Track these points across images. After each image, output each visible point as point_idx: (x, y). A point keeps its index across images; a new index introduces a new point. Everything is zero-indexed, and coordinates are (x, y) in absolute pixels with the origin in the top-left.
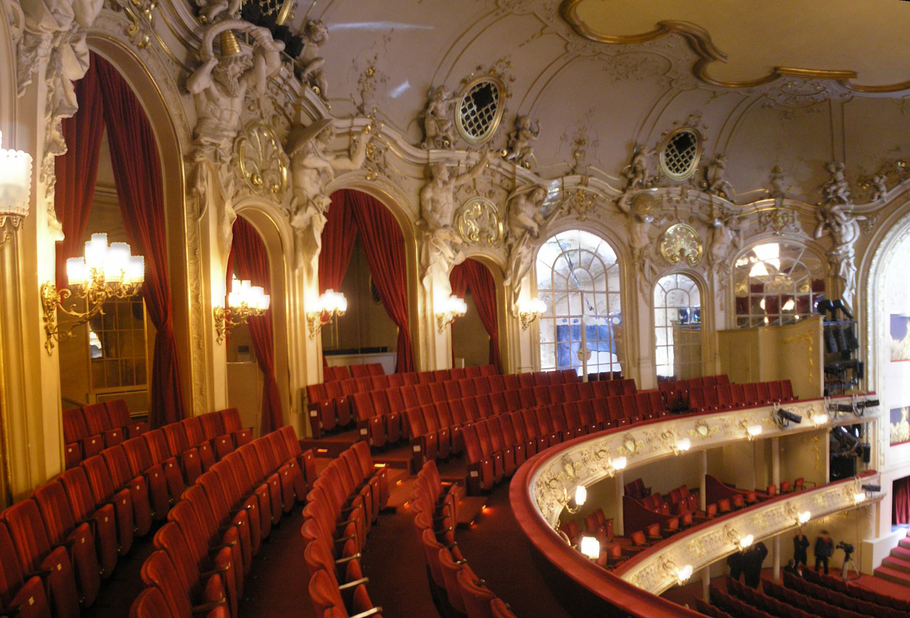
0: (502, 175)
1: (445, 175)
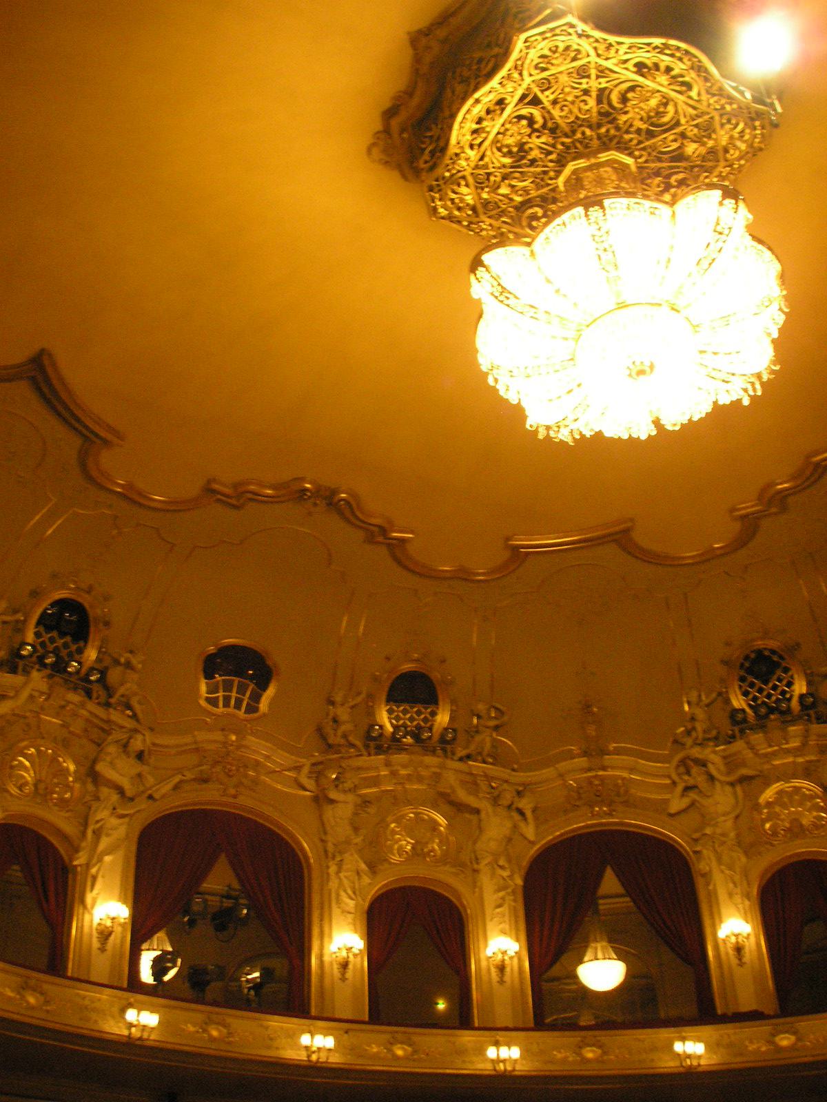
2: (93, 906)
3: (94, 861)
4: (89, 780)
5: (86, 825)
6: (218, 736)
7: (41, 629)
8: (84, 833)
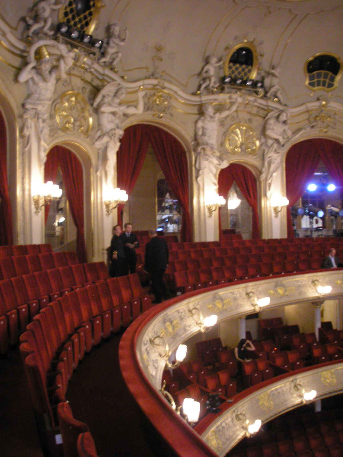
0: (258, 107)
1: (210, 110)
2: (270, 198)
3: (269, 176)
4: (262, 137)
5: (263, 159)
6: (317, 104)
7: (231, 64)
8: (263, 164)
